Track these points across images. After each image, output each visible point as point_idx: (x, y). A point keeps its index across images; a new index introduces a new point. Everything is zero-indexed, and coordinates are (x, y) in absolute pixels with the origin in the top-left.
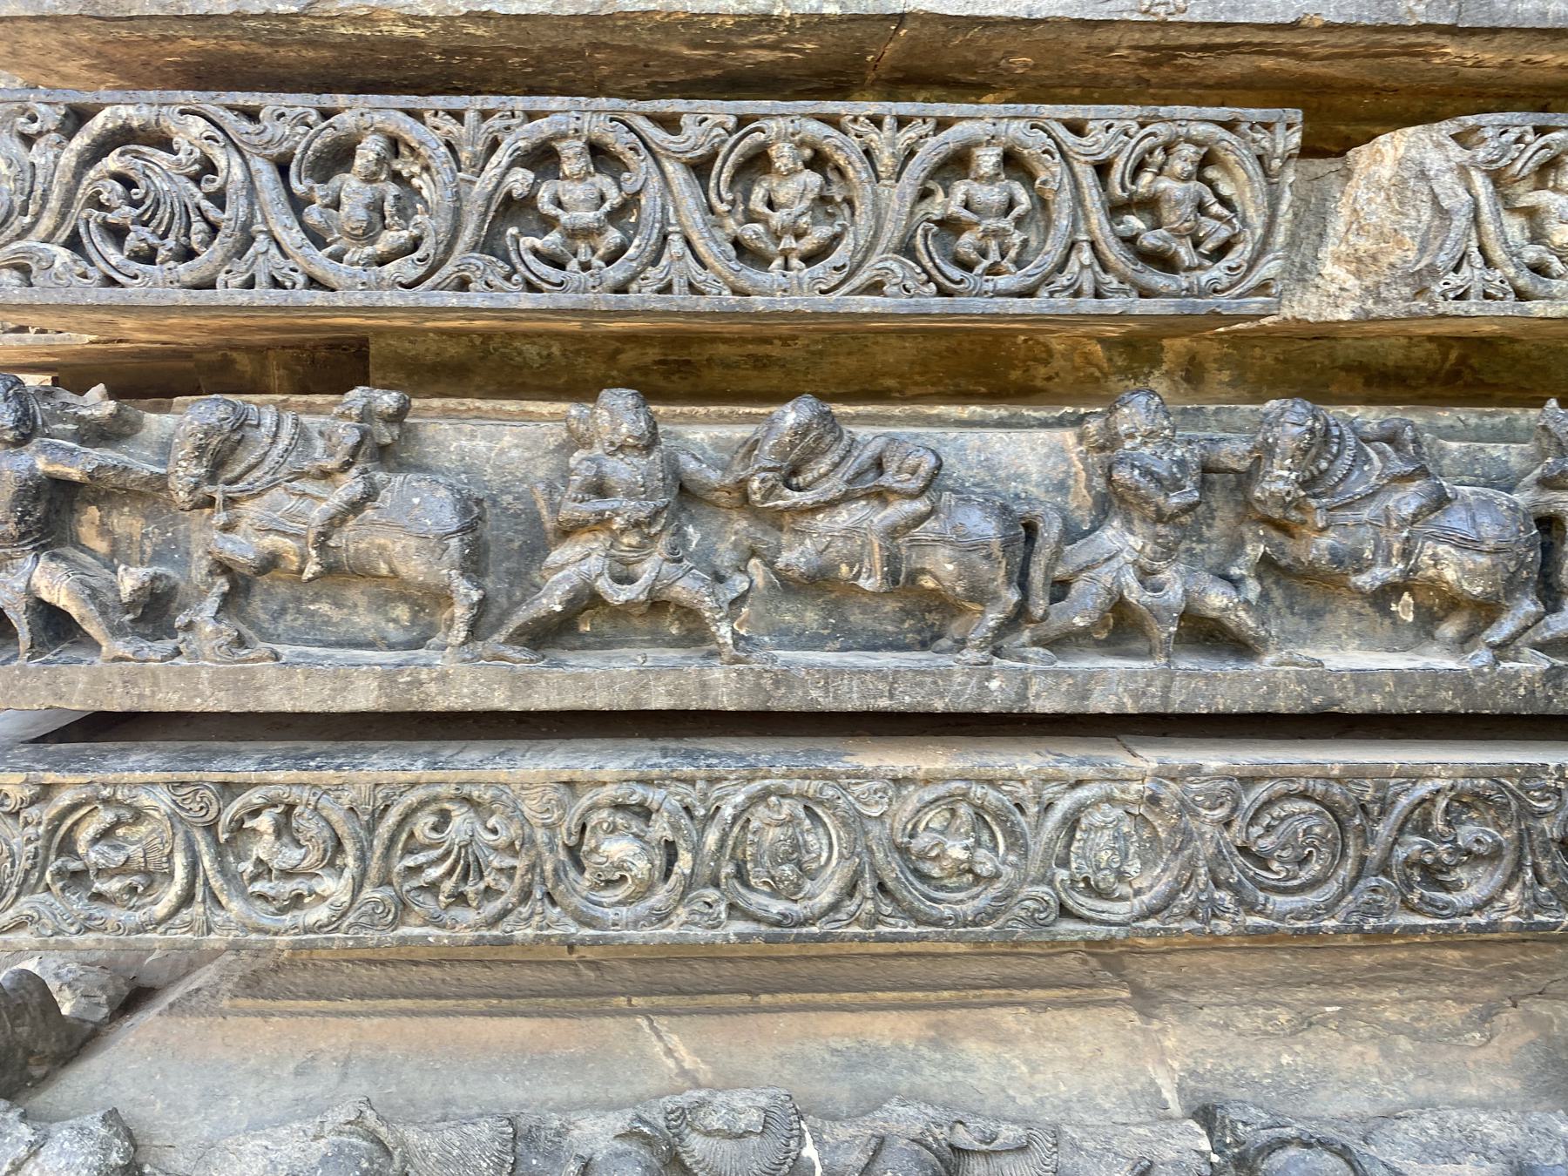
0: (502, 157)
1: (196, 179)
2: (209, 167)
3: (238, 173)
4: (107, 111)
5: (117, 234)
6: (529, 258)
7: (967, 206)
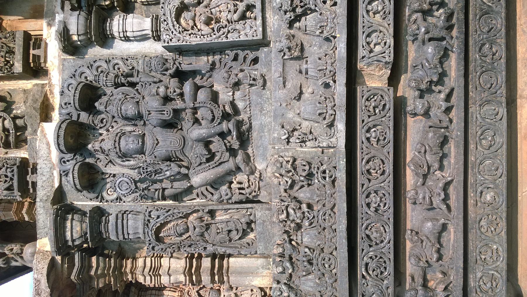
0: (369, 212)
1: (373, 260)
2: (371, 258)
3: (372, 253)
4: (364, 273)
5: (382, 273)
6: (385, 208)
7: (375, 138)
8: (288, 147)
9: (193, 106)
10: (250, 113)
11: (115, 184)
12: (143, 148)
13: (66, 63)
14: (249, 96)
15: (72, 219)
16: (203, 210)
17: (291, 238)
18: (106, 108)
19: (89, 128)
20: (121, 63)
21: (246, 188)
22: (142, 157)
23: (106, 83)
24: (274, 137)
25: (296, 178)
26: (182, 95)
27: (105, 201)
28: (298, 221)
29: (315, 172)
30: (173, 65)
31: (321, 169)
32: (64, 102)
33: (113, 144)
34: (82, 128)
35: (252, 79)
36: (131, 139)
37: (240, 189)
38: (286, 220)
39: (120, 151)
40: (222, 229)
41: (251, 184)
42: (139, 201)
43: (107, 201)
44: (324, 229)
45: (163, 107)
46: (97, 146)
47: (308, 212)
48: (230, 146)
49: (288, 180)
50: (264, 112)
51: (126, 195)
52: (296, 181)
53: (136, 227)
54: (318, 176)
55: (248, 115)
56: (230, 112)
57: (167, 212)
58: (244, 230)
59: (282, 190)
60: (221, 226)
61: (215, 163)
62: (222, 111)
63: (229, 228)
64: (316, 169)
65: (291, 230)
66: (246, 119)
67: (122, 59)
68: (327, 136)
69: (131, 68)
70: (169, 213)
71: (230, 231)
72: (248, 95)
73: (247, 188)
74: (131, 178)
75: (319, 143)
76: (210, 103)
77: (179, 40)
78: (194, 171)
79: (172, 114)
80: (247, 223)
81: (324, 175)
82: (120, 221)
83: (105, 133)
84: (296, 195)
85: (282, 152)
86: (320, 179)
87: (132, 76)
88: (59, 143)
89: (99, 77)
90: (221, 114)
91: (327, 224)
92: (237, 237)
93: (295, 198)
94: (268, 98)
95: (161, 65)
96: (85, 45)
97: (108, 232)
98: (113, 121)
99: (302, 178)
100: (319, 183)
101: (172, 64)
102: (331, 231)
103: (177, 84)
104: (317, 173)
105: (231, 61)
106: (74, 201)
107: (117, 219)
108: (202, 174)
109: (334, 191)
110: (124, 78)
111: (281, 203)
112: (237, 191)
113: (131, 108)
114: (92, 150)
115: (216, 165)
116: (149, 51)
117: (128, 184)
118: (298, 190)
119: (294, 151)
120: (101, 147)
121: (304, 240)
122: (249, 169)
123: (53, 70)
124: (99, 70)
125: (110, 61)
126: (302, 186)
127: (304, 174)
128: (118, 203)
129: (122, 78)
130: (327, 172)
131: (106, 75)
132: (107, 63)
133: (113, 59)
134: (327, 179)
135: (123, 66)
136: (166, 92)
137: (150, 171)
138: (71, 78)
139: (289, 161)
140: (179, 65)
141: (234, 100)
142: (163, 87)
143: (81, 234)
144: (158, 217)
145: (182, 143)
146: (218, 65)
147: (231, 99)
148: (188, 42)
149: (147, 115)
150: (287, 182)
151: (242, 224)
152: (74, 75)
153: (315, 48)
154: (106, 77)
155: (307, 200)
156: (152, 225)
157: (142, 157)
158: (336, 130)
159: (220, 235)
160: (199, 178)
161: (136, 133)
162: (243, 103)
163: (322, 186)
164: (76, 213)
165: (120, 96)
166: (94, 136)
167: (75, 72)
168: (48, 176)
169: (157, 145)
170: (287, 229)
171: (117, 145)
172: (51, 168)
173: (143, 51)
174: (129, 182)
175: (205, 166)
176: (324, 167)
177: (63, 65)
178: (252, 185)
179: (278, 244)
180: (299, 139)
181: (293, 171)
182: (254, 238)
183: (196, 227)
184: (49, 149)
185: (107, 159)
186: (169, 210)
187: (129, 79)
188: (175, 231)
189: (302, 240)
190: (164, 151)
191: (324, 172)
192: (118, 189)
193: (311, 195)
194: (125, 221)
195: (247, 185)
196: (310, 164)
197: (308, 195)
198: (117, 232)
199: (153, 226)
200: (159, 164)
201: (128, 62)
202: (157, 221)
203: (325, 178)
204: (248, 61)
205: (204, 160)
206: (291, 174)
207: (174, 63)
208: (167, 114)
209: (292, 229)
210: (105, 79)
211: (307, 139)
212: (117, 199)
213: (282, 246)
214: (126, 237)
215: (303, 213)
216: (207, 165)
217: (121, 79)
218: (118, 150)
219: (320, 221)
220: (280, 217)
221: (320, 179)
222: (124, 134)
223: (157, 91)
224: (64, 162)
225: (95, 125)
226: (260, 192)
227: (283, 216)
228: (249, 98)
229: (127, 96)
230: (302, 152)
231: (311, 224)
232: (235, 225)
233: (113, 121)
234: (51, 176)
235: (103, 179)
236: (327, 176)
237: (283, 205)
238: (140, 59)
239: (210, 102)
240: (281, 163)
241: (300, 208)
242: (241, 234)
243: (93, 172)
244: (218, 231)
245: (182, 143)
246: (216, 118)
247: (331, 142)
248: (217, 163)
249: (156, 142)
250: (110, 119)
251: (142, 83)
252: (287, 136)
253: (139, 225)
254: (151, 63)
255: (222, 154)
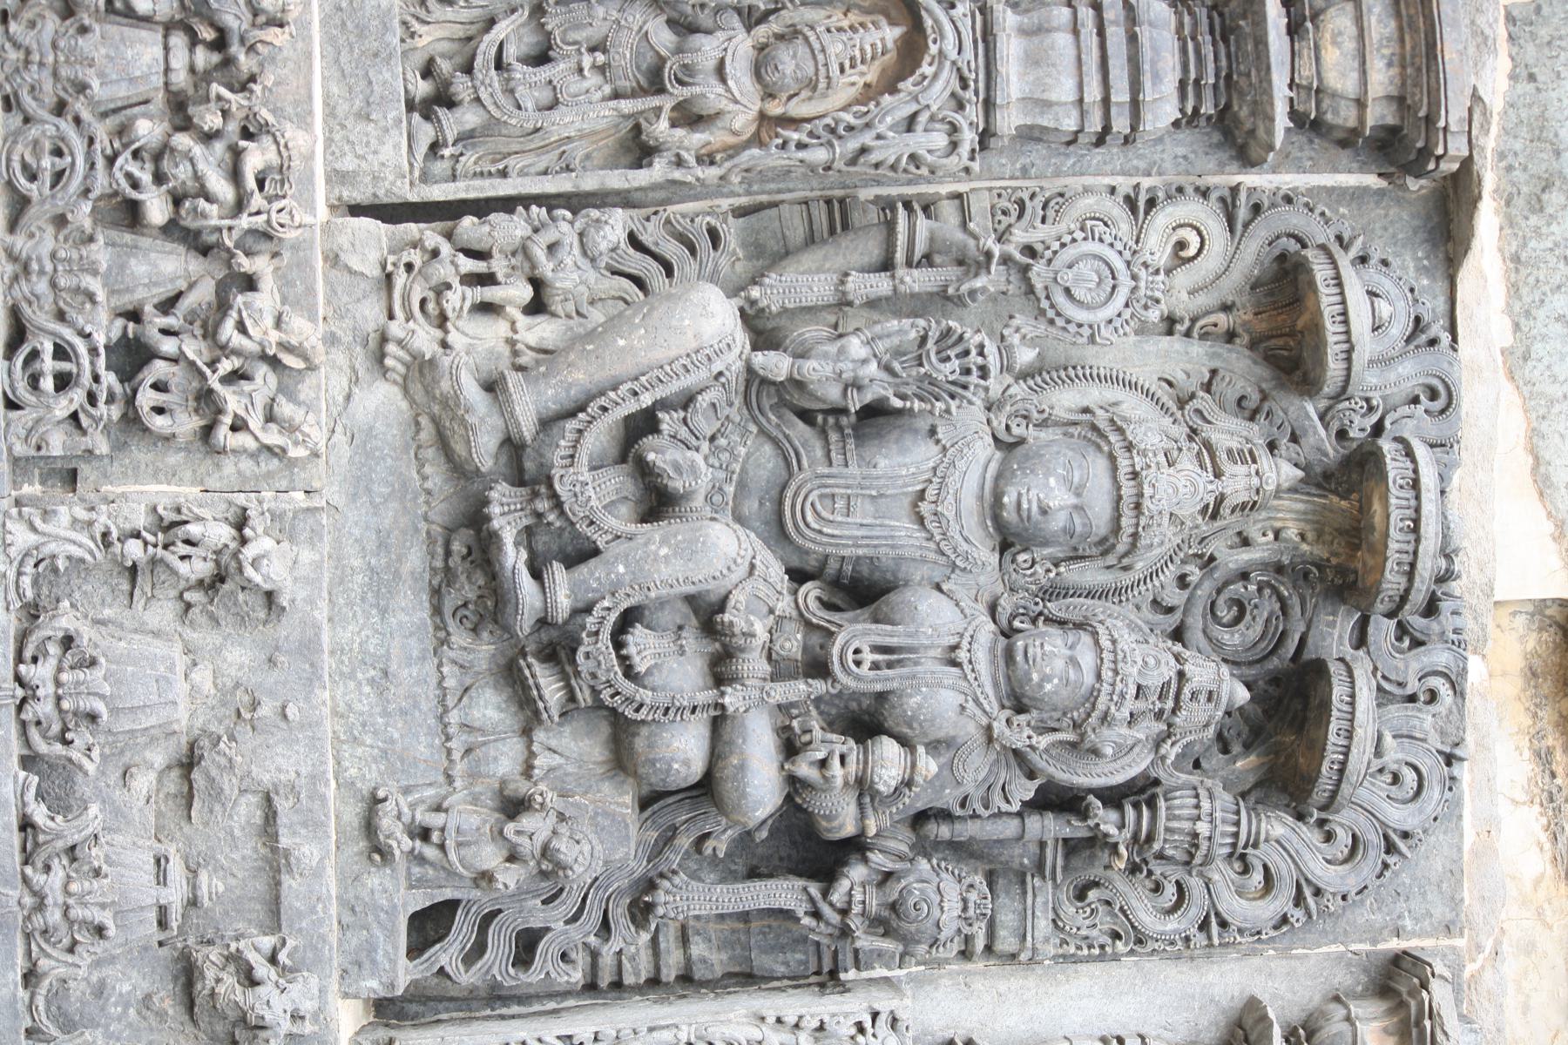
8: (241, 499)
9: (723, 694)
10: (440, 665)
11: (1134, 290)
12: (999, 477)
13: (1440, 911)
14: (449, 752)
15: (1361, 104)
16: (679, 162)
17: (216, 58)
18: (1181, 675)
19: (1306, 575)
20: (1146, 915)
21: (456, 283)
22: (1008, 427)
23: (1197, 807)
24: (313, 546)
25: (193, 349)
26: (791, 748)
27: (1214, 196)
28: (182, 141)
29: (109, 379)
30: (849, 903)
31: (77, 396)
32: (1440, 708)
33: (1147, 491)
34: (1341, 571)
35: (435, 837)
36: (1057, 522)
37: (487, 279)
38: (243, 143)
39: (1112, 458)
40: (581, 70)
41: (431, 306)
42: (1033, 196)
43: (1204, 193)
44: (60, 108)
45: (878, 687)
46: (1238, 481)
47: (135, 185)
48: (535, 495)
49: (237, 340)
50: (372, 673)
51: (1079, 235)
52: (198, 332)
53: (1037, 63)
54: (92, 363)
55: (452, 654)
56: (538, 668)
57: (864, 150)
58: (468, 69)
59: (267, 283)
60: (586, 84)
61: (604, 409)
62: (577, 674)
63: (545, 72)
64: (102, 397)
65: (219, 98)
66: (460, 638)
67: (1139, 942)
68: (53, 557)
69: (1092, 895)
70: (853, 145)
71: (541, 58)
72: (456, 756)
73: (449, 286)
74: (1052, 322)
75: (90, 524)
76: (637, 710)
77: (821, 1028)
78: (718, 366)
79: (835, 651)
80: (451, 104)
81: (65, 366)
82: (1121, 95)
83: (1218, 547)
84: (195, 265)
85: (269, 475)
86: (81, 347)
87: (1071, 847)
88: (1410, 494)
89: (1236, 835)
90: (580, 658)
91: (49, 127)
92: (501, 30)
93: (205, 251)
94: (355, 740)
95: (911, 902)
96: (1333, 1006)
97: (1182, 40)
98: (1178, 616)
99: (168, 346)
100: (88, 329)
101: (856, 909)
102: (27, 100)
103: (820, 805)
104: (96, 378)
105: (548, 929)
106: (1381, 193)
107: (1135, 105)
108: (673, 353)
109: (16, 292)
110: (1106, 835)
111: (268, 222)
112: (498, 266)
113: (1046, 678)
114: (1265, 461)
115: (602, 401)
116: (1002, 986)
117: (1067, 291)
118: (191, 286)
119: (212, 483)
120: (1218, 474)
121: (158, 51)
122: (436, 381)
123: (1537, 882)
124: (1257, 877)
125: (1204, 926)
126: (168, 305)
127: (159, 369)
128: (1146, 183)
129: (1113, 830)
130: (48, 384)
131: (1197, 846)
132: (1217, 914)
133: (1187, 939)
134: (48, 348)
135: (1134, 903)
136: (866, 762)
137: (948, 359)
138: (1406, 835)
139: (234, 428)
140: (826, 910)
141: (527, 732)
142: (881, 788)
143: (1316, 27)
144: (910, 124)
145: (793, 506)
146: (619, 915)
147: (539, 736)
148: (771, 1020)
149: (965, 645)
150: (241, 328)
151: (478, 100)
152: (1390, 848)
153: (126, 988)
154: (1196, 835)
155: (145, 242)
156: (939, 84)
157: (1008, 427)
158: (12, 588)
159: (588, 39)
160: (690, 334)
161: (1047, 551)
162: (476, 714)
163: (72, 314)
164: (1355, 132)
165: (1108, 739)
166: (1277, 534)
167: (1386, 866)
168: (1541, 314)
169: (921, 495)
170: (235, 100)
171: (1128, 489)
172: (1526, 357)
173: (1031, 982)
174: (1060, 299)
175: (660, 393)
176: (63, 406)
177: (1455, 902)
178: (423, 302)
179: (281, 26)
180: (188, 542)
181: (214, 382)
182: (416, 26)
183: (714, 81)
184: (1537, 458)
185: (1198, 412)
186: (853, 162)
187: (1074, 828)
188: (820, 57)
189: (166, 48)
190: (883, 463)
191: (63, 382)
192: (1119, 264)
193: (122, 267)
194: (1093, 93)
195: (455, 299)
196: (131, 420)
197: (139, 268)
198: (1133, 39)
199: (936, 76)
200: (903, 397)
201: (1105, 922)
202: (914, 107)
203: (61, 353)
204: (462, 932)
205: (668, 421)
206: (226, 366)
207: (844, 912)
208: (857, 651)
209: (213, 95)
210: (1203, 828)
211: (150, 538)
212: (1151, 203)
213: (262, 19)
214: (1086, 14)
215: (159, 178)
216: (647, 400)
217: (1121, 826)
218: (1124, 464)
219: (78, 144)
220: (272, 156)
221: (81, 347)
222: (1105, 546)
223: (914, 765)
224: (1433, 395)
225: (1275, 590)
226: (384, 267)
227: (256, 158)
228: (448, 739)
229: (1070, 736)
230: (172, 476)
231: (122, 131)
232: (512, 91)
233: (1178, 616)
234: (1528, 314)
235: (1226, 308)
236: (48, 364)
237: (258, 213)
238: (1047, 940)
239: (640, 716)
240: (270, 418)
241: (177, 201)
242: (482, 47)
243: (1280, 342)
244: (600, 58)
245: (793, 506)
246: (605, 636)
247: (33, 529)
248: (593, 408)
249: (925, 508)
250: (1196, 622)
251: (1005, 807)
252: (249, 552)
253: (1022, 75)
254: (965, 909)
255: (572, 456)
